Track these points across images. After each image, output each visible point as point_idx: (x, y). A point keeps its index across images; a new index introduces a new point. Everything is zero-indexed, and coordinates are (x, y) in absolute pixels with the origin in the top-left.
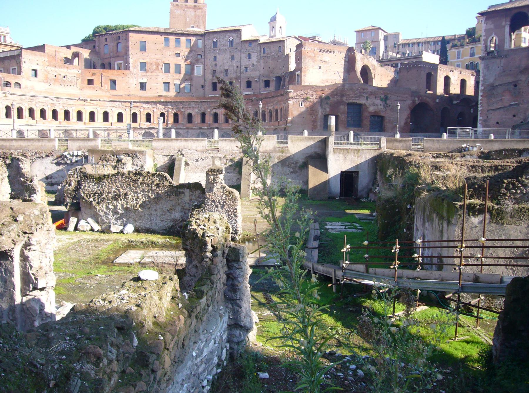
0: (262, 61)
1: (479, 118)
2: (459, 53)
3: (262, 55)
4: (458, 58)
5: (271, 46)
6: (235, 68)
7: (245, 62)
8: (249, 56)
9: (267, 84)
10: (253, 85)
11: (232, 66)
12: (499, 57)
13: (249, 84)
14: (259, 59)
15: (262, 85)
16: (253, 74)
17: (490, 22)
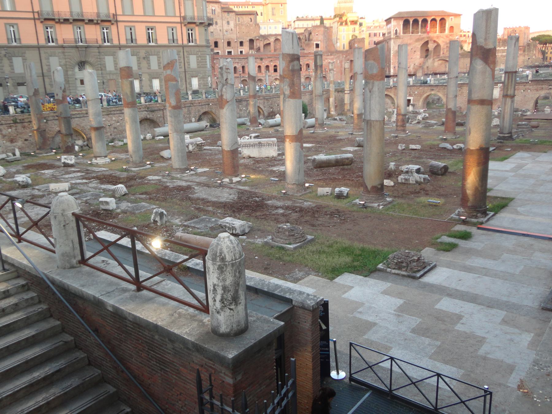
0: (238, 27)
1: (392, 66)
2: (344, 29)
3: (237, 22)
4: (344, 32)
5: (244, 17)
6: (219, 31)
7: (226, 27)
8: (228, 23)
9: (241, 43)
10: (232, 44)
11: (216, 29)
12: (400, 38)
13: (229, 44)
14: (236, 25)
15: (239, 44)
16: (233, 37)
17: (395, 22)
